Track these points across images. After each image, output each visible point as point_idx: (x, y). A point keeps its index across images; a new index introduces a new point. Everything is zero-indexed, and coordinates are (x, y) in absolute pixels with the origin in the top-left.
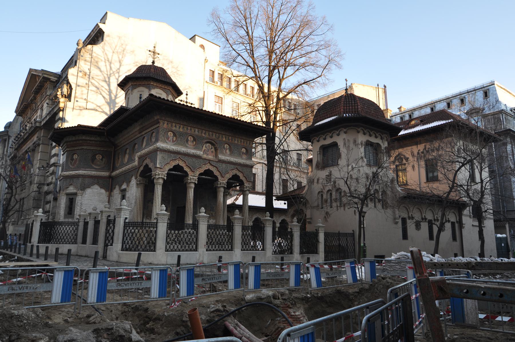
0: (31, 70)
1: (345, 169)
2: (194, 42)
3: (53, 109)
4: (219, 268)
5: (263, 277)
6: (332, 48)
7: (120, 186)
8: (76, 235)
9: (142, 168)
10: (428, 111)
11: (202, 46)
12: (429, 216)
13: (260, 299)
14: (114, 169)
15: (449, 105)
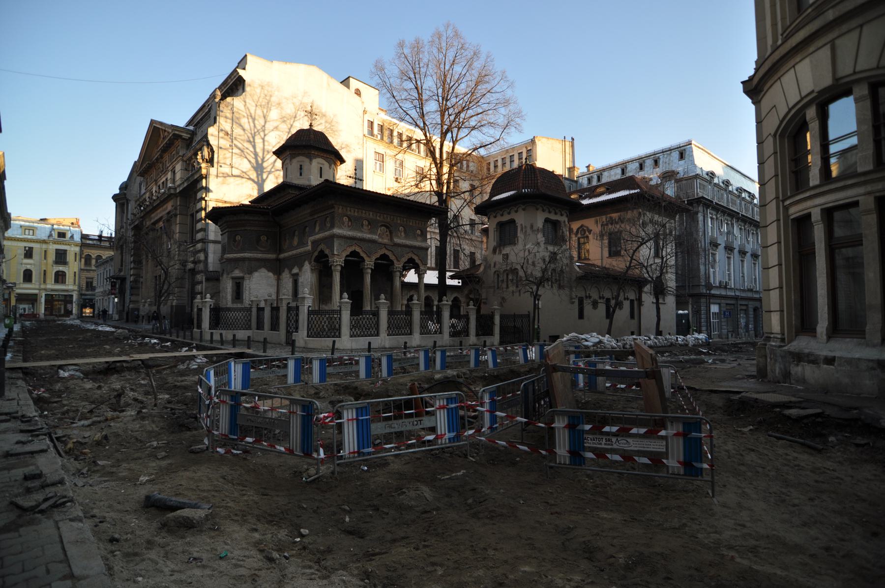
0: (152, 122)
1: (521, 254)
2: (348, 87)
3: (192, 175)
4: (405, 353)
5: (448, 360)
6: (511, 107)
7: (290, 270)
8: (250, 321)
9: (316, 254)
10: (616, 175)
11: (358, 93)
12: (607, 294)
13: (446, 378)
14: (281, 251)
15: (641, 167)
